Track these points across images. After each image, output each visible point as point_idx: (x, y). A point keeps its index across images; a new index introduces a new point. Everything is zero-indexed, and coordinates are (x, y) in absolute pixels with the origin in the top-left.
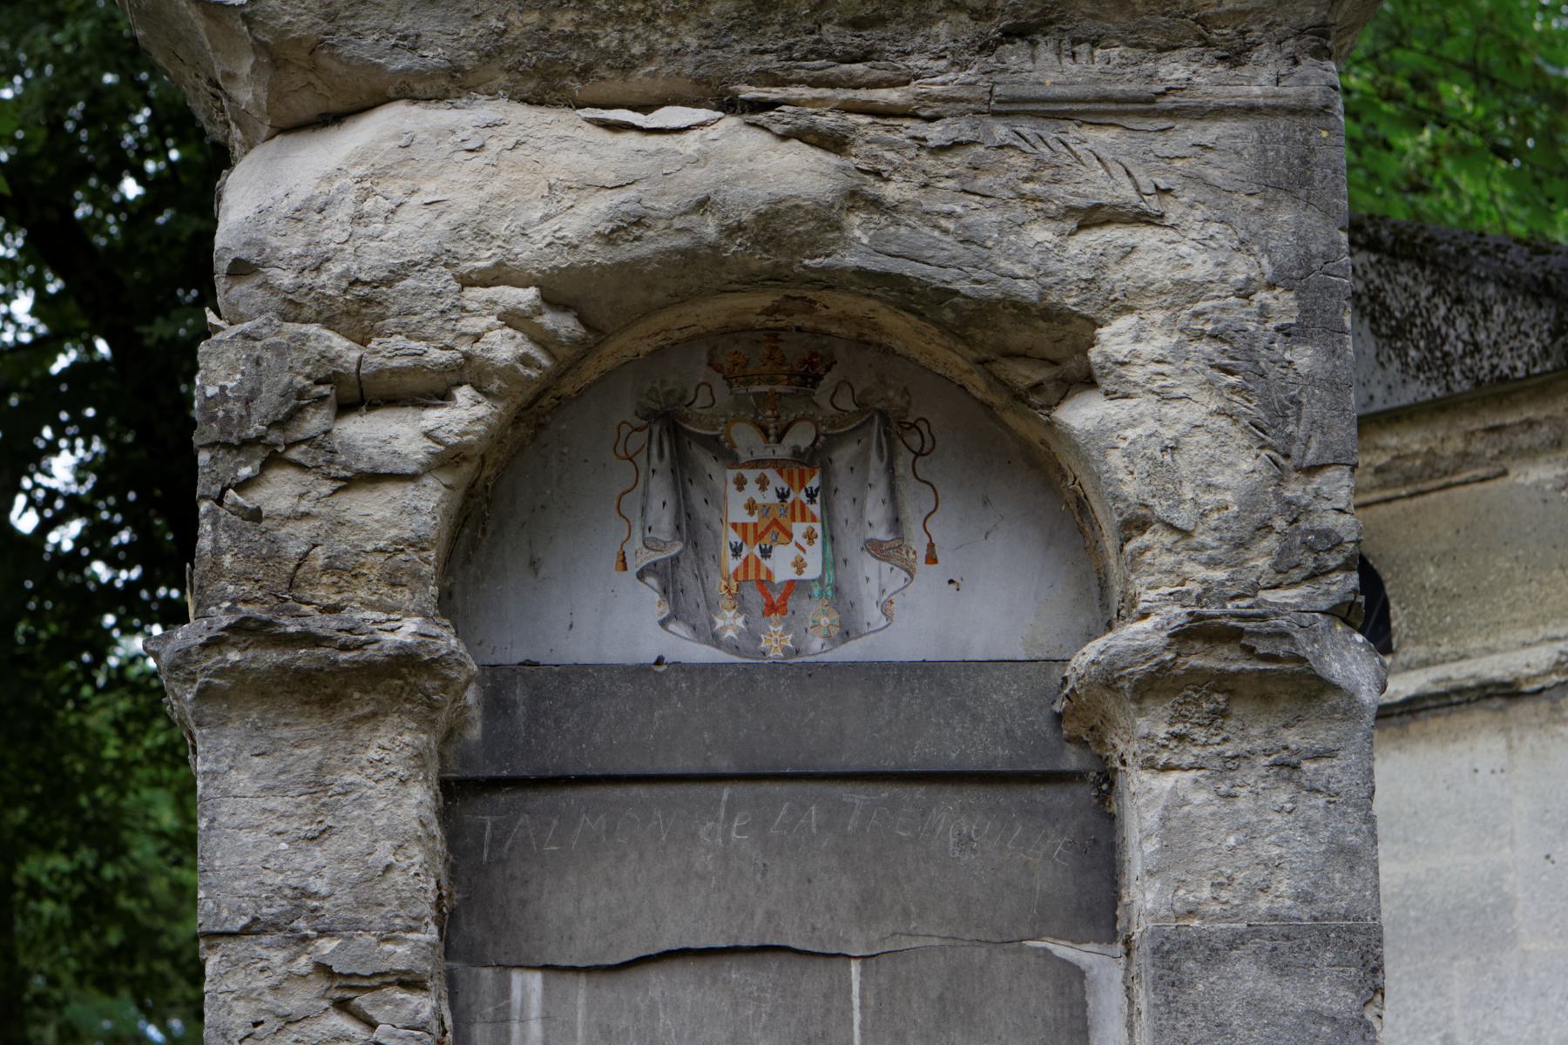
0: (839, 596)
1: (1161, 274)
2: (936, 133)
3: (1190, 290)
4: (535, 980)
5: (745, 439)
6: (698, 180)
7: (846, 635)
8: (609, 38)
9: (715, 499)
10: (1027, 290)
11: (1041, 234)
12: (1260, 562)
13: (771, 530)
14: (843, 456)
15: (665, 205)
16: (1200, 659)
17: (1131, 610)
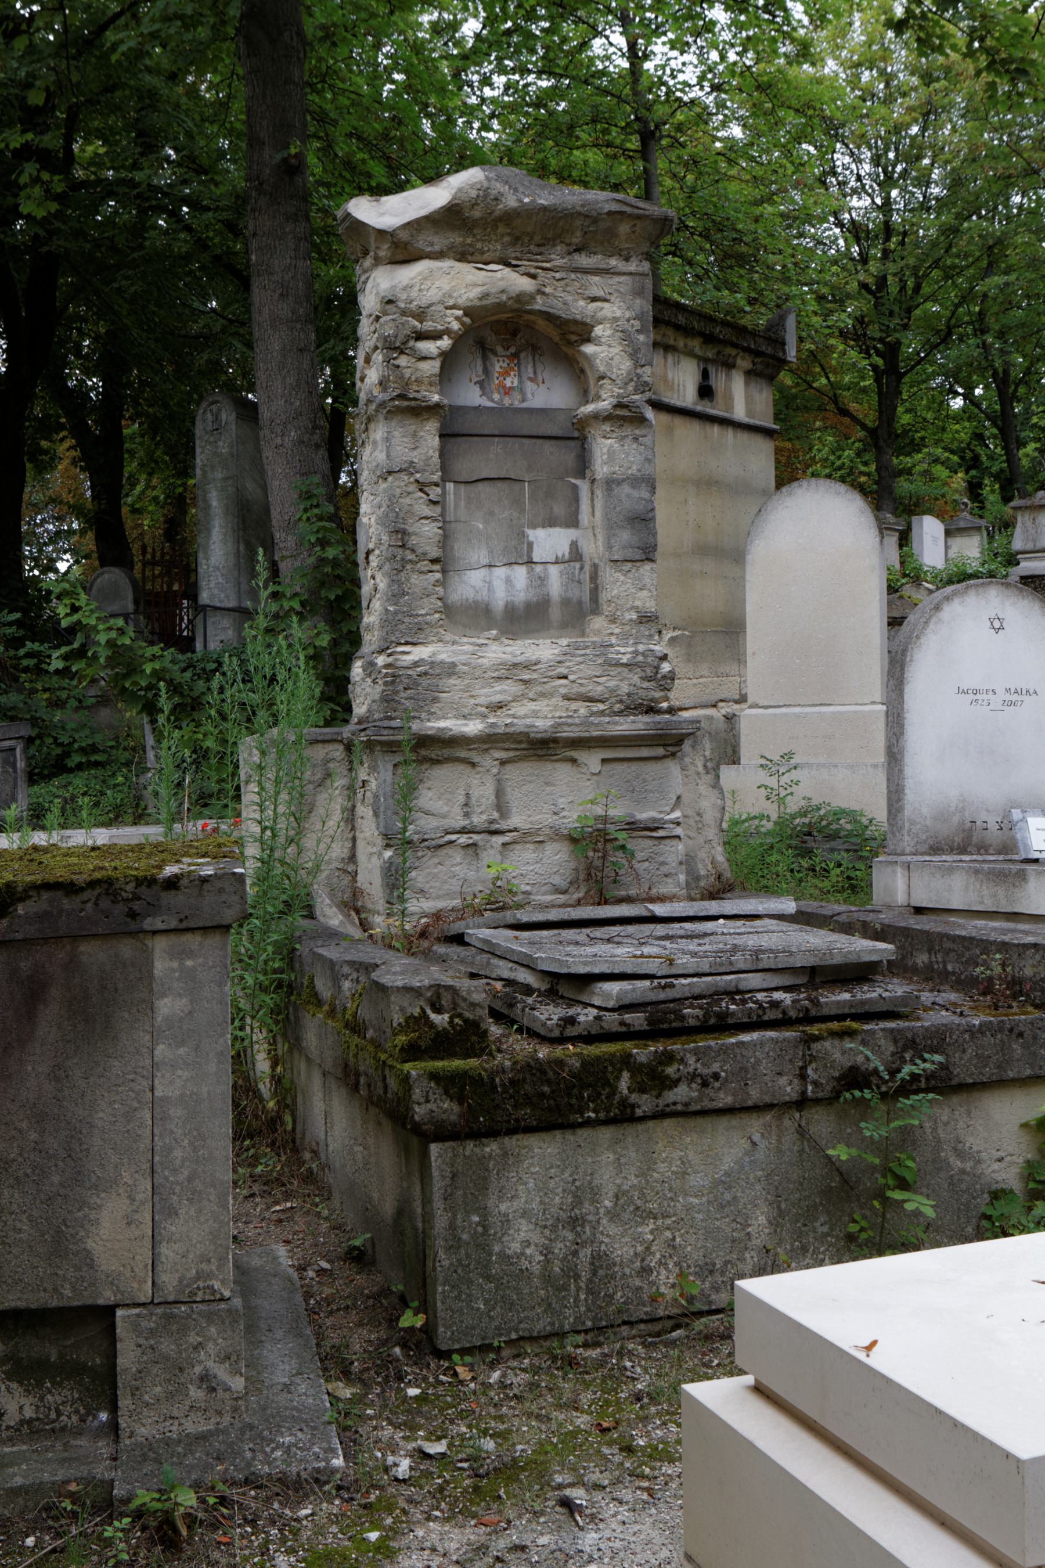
0: (522, 391)
1: (609, 315)
2: (558, 275)
3: (615, 319)
4: (452, 485)
5: (500, 350)
6: (502, 285)
7: (524, 400)
8: (479, 245)
9: (493, 365)
10: (579, 317)
11: (582, 303)
12: (630, 388)
13: (506, 373)
14: (523, 355)
15: (494, 291)
16: (619, 412)
17: (598, 398)
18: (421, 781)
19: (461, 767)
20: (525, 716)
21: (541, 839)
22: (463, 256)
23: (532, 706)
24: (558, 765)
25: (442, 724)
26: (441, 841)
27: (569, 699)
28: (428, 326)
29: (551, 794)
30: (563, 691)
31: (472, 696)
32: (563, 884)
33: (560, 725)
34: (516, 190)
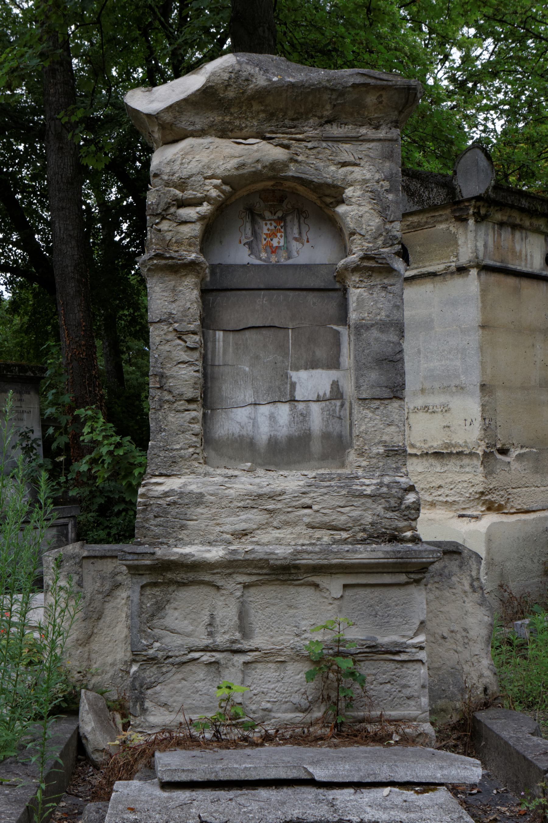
0: (287, 249)
1: (359, 177)
2: (310, 145)
3: (365, 181)
4: (221, 333)
5: (267, 214)
6: (257, 155)
7: (289, 257)
8: (237, 123)
9: (261, 228)
10: (329, 181)
11: (333, 168)
12: (380, 242)
13: (273, 235)
14: (289, 218)
15: (250, 161)
16: (366, 264)
17: (351, 253)
18: (168, 601)
19: (206, 590)
20: (269, 543)
21: (282, 659)
22: (223, 134)
23: (276, 534)
24: (301, 589)
25: (187, 550)
26: (185, 659)
27: (313, 528)
28: (189, 194)
29: (294, 616)
30: (307, 520)
31: (218, 524)
32: (304, 703)
33: (299, 552)
34: (266, 71)
